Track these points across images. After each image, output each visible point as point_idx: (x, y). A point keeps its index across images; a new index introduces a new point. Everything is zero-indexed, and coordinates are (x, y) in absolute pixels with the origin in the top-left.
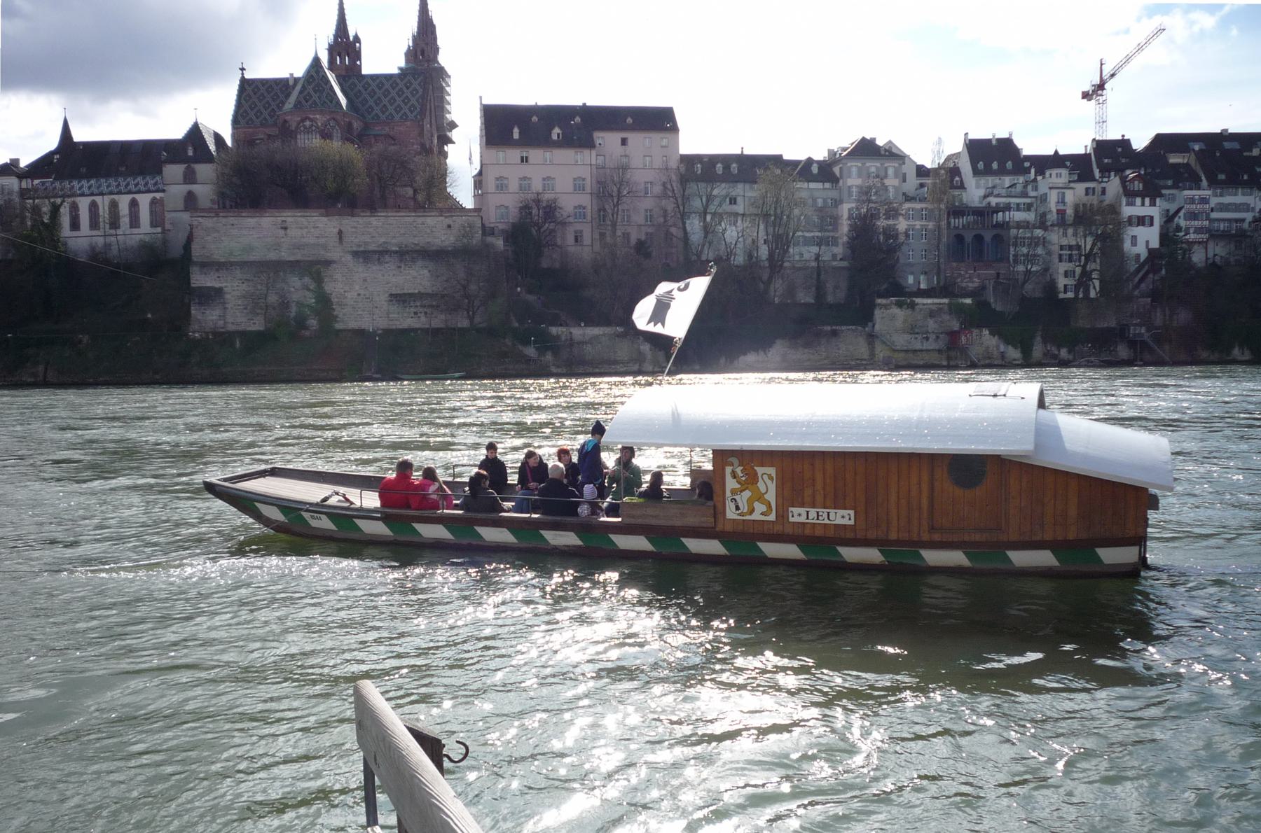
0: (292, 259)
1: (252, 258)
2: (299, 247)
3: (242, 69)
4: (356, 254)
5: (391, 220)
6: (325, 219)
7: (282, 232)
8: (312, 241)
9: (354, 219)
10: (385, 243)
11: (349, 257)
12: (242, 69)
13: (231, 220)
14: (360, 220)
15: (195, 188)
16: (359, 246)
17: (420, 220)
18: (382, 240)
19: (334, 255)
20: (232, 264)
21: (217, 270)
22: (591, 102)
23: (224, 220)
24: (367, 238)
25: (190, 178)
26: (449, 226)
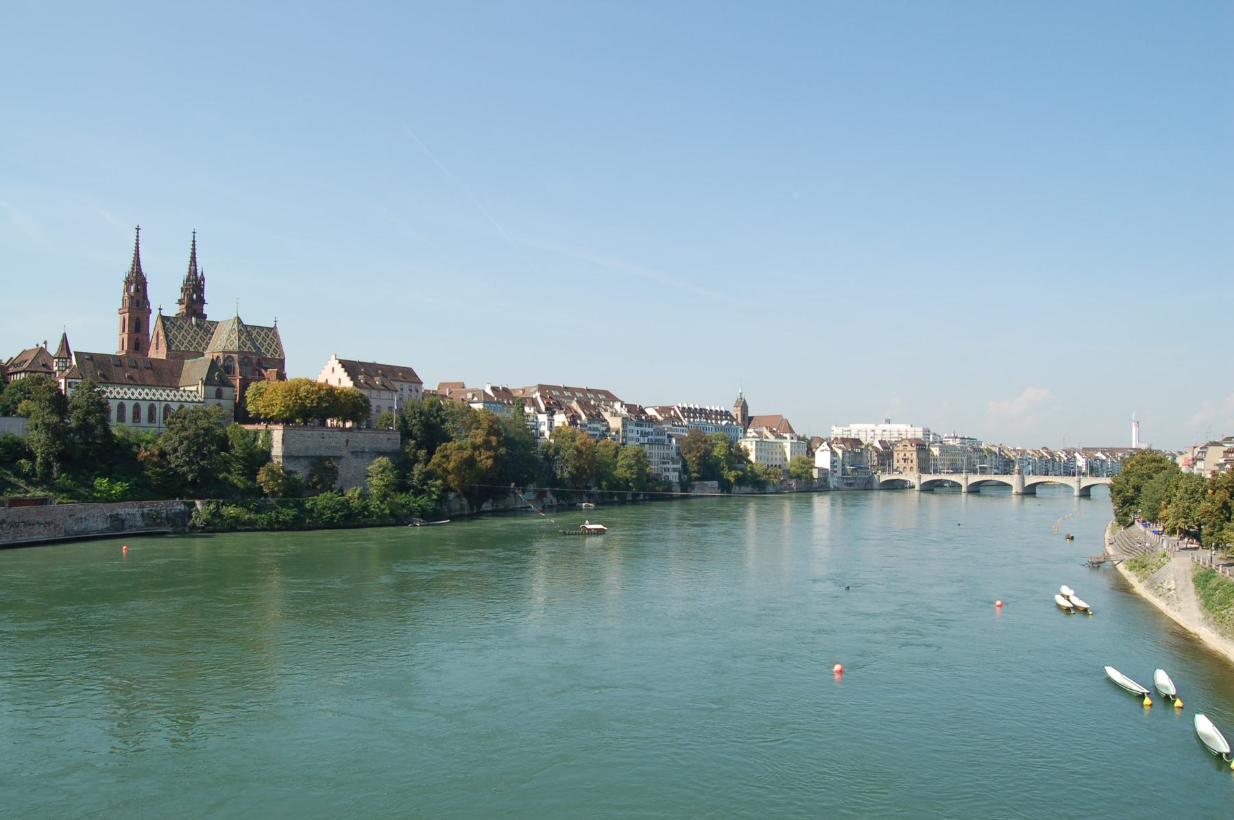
0: (326, 455)
1: (309, 454)
2: (329, 448)
3: (160, 309)
4: (353, 453)
5: (366, 435)
6: (340, 433)
7: (322, 439)
8: (334, 445)
9: (352, 433)
10: (364, 447)
11: (350, 454)
12: (160, 309)
13: (301, 432)
14: (355, 434)
15: (221, 401)
16: (353, 448)
17: (378, 435)
18: (363, 445)
19: (344, 453)
20: (300, 457)
21: (294, 460)
22: (378, 362)
23: (297, 432)
24: (356, 444)
25: (219, 395)
26: (388, 439)
